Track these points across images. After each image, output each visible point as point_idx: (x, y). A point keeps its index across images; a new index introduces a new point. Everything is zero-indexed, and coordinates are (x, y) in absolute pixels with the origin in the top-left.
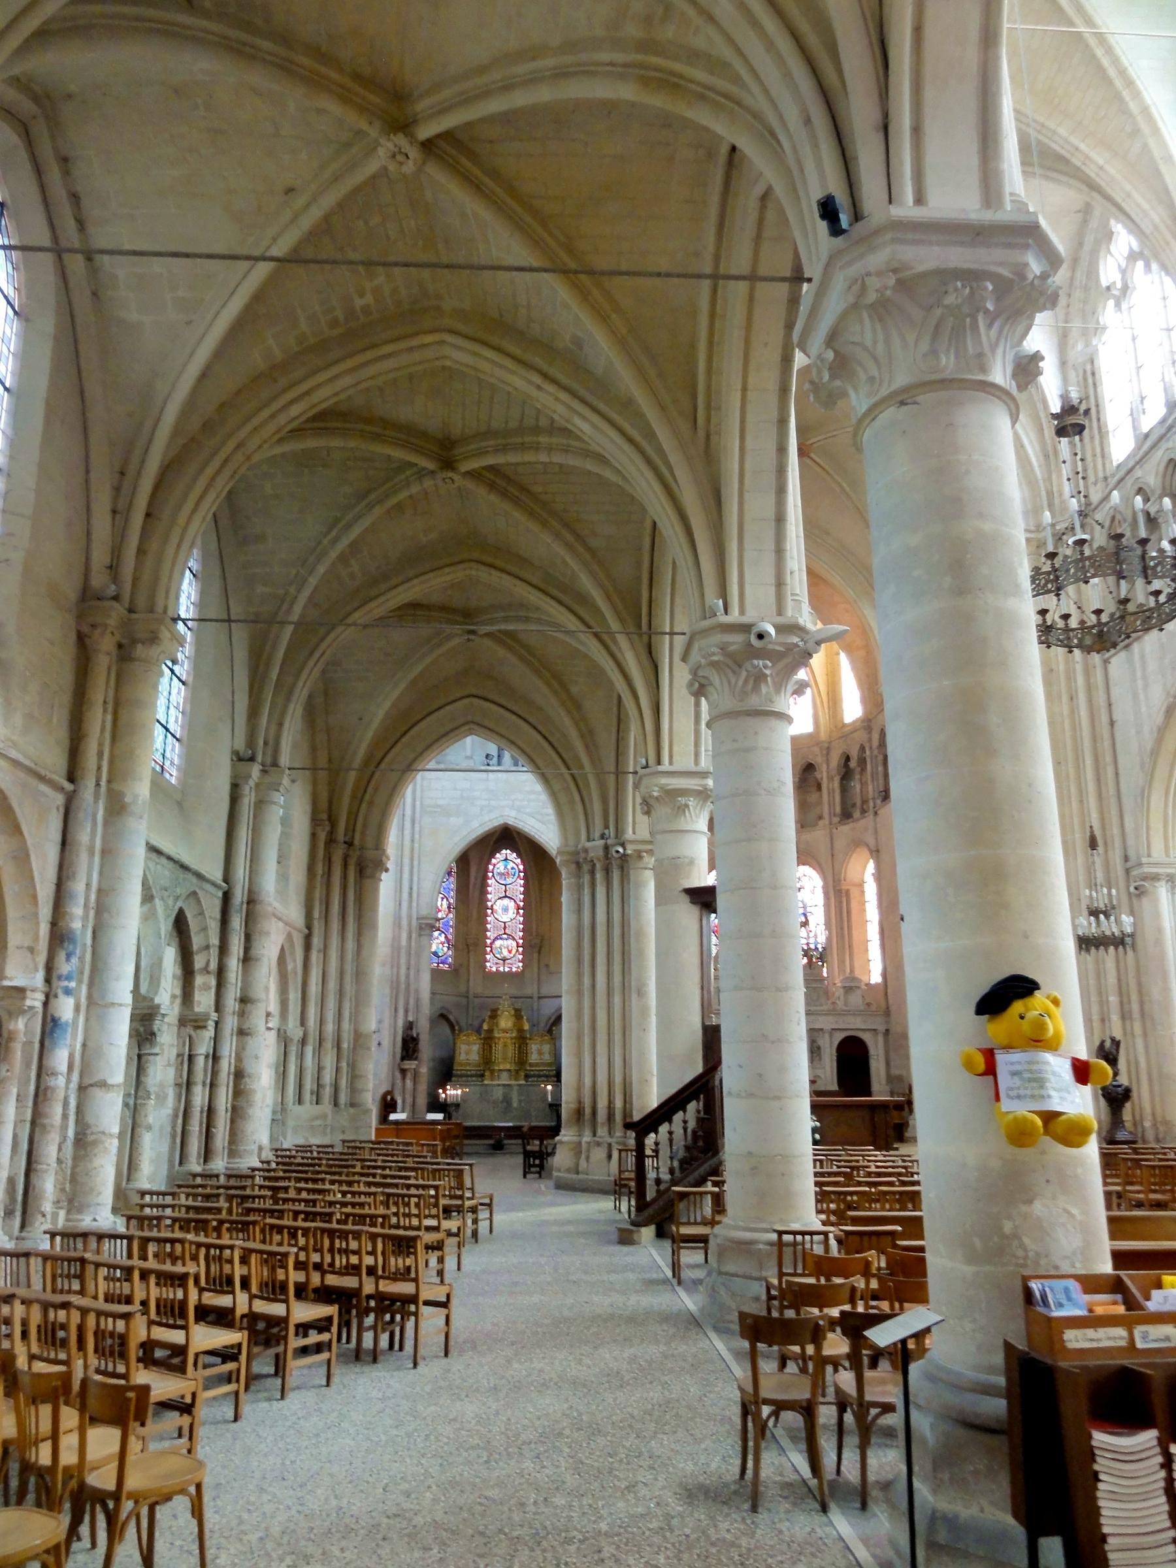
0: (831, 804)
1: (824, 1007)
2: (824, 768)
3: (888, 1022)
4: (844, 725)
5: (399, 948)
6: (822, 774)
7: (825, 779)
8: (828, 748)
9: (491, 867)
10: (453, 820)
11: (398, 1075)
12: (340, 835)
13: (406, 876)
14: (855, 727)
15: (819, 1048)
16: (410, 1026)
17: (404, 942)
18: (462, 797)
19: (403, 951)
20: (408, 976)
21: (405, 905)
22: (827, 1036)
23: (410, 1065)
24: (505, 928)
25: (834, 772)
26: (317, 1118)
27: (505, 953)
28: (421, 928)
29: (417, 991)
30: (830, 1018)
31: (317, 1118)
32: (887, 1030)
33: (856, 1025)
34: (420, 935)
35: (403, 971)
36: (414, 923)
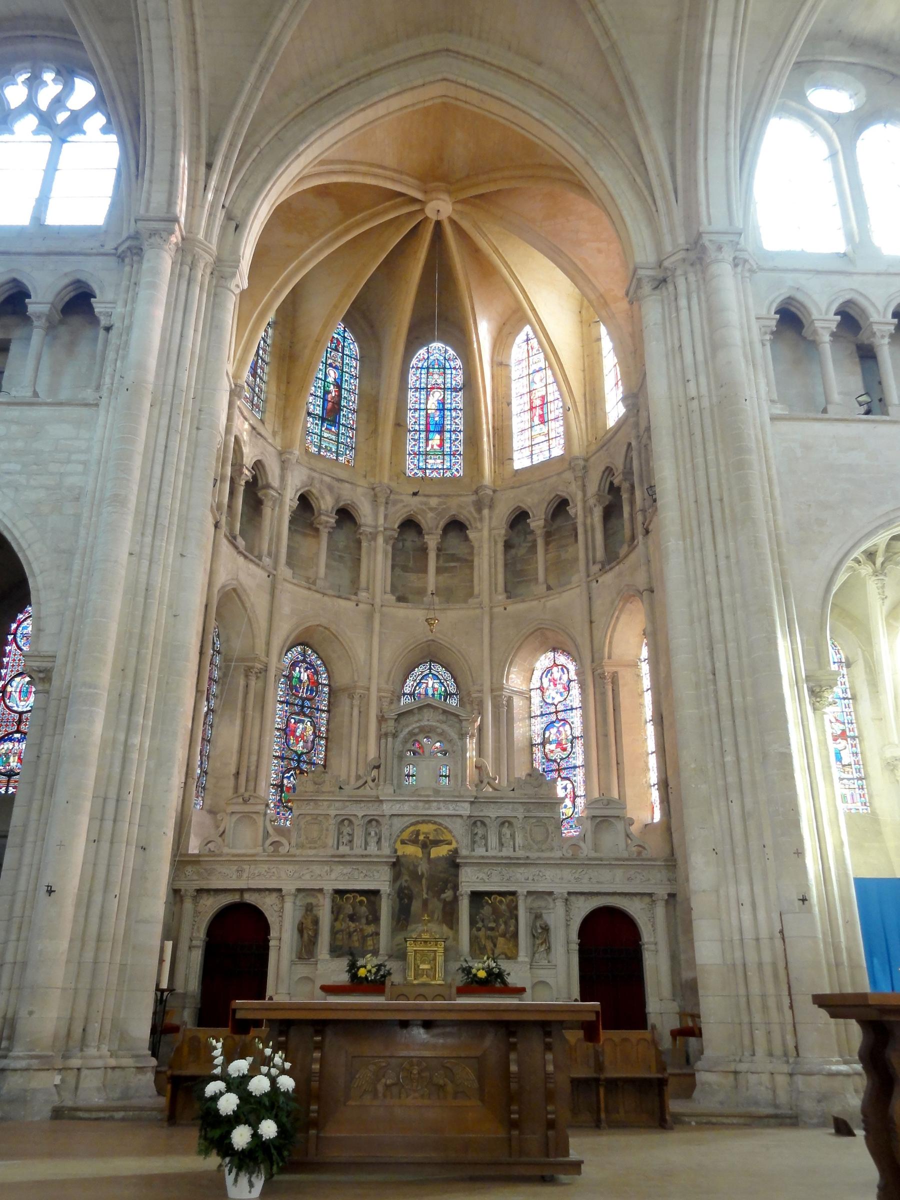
0: (590, 547)
1: (558, 854)
2: (579, 496)
3: (672, 880)
4: (607, 432)
6: (576, 509)
7: (580, 513)
8: (585, 467)
9: (14, 626)
14: (622, 423)
15: (546, 929)
22: (560, 904)
24: (20, 722)
25: (592, 502)
27: (14, 763)
30: (566, 873)
32: (672, 896)
33: (612, 885)
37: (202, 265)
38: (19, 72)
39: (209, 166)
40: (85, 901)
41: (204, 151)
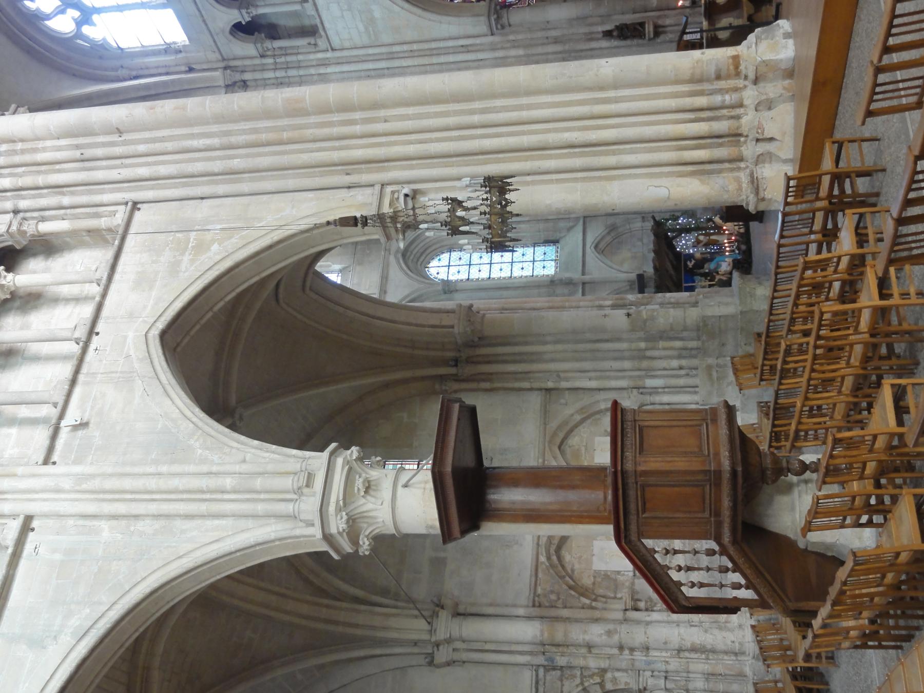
5: (528, 56)
10: (377, 14)
11: (662, 38)
12: (453, 371)
13: (451, 58)
16: (608, 34)
17: (521, 52)
18: (350, 9)
19: (530, 52)
20: (556, 41)
21: (480, 56)
23: (649, 29)
26: (710, 376)
28: (503, 27)
29: (571, 22)
31: (710, 375)
34: (510, 25)
35: (551, 48)
36: (496, 39)
38: (28, 9)
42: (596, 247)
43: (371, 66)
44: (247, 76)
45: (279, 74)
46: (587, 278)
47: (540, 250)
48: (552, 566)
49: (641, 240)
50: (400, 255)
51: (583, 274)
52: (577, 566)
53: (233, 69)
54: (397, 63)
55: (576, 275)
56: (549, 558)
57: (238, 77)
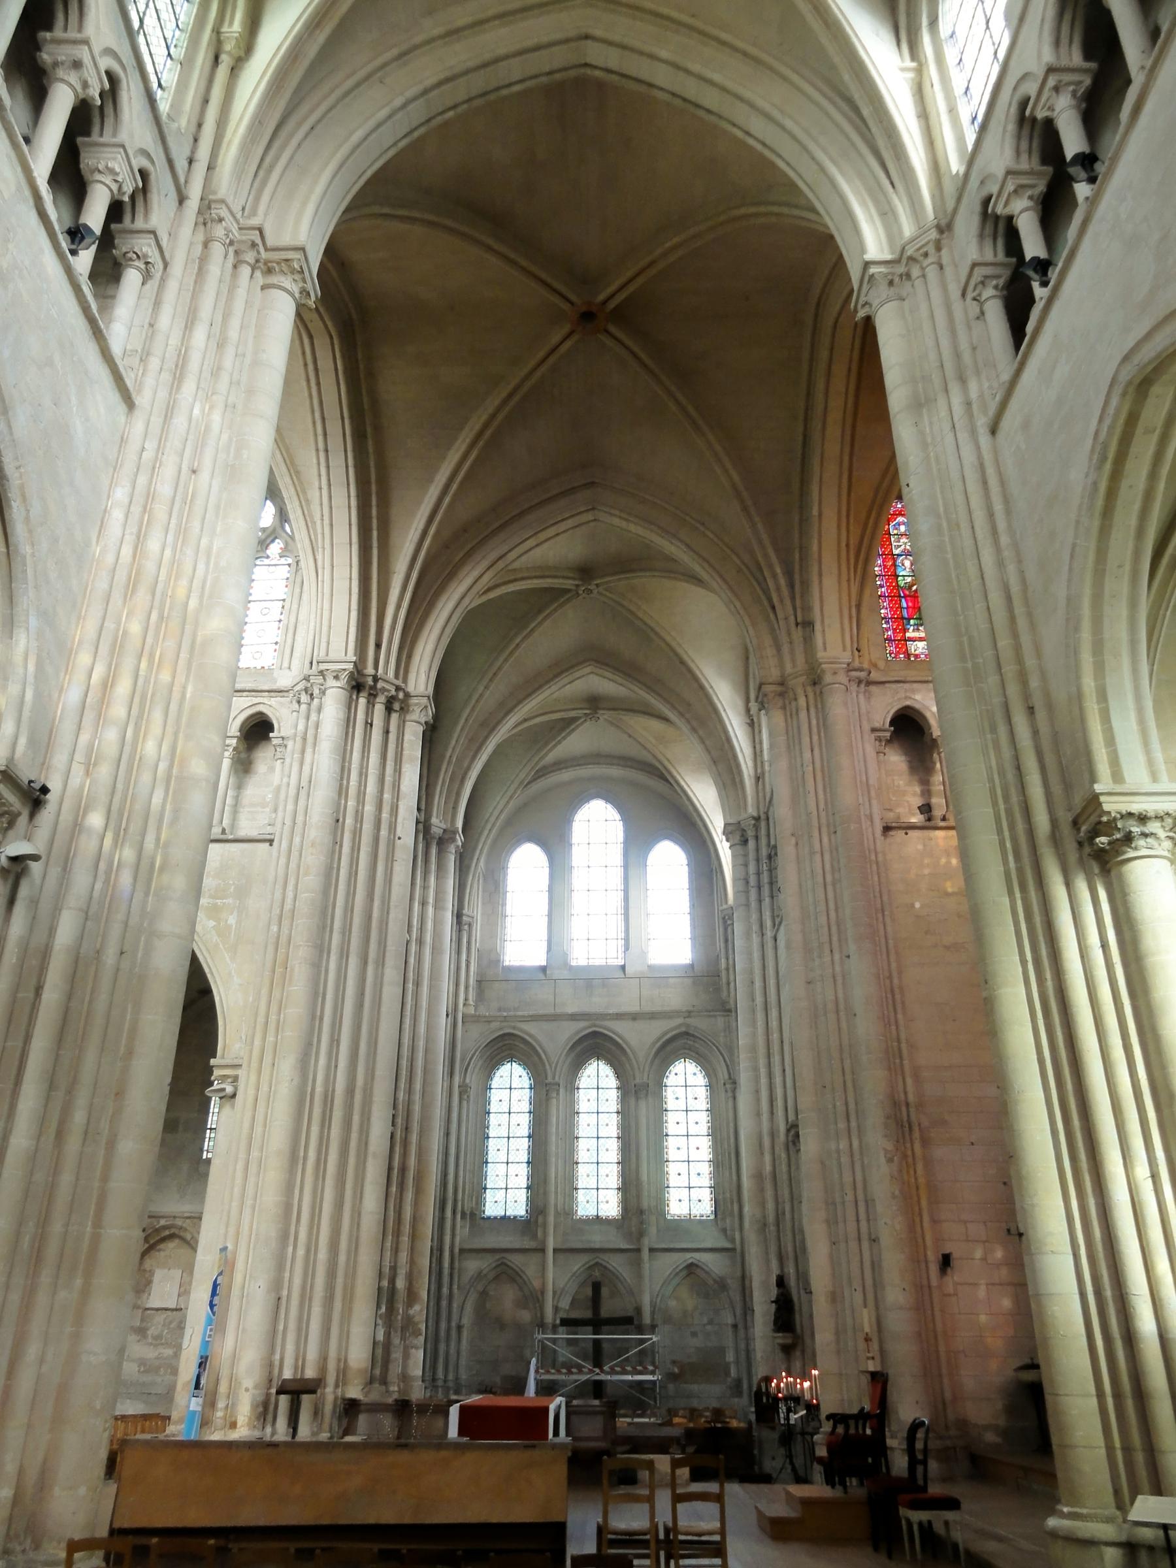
13: (764, 1081)
16: (781, 1282)
37: (800, 691)
39: (773, 608)
40: (834, 1297)
41: (766, 603)
42: (692, 1264)
43: (758, 984)
44: (751, 844)
45: (753, 880)
46: (645, 1254)
47: (706, 1195)
48: (157, 1231)
49: (711, 1322)
50: (683, 1029)
51: (651, 1250)
52: (162, 1254)
53: (757, 828)
54: (760, 1016)
55: (646, 1243)
56: (165, 1228)
57: (750, 833)
